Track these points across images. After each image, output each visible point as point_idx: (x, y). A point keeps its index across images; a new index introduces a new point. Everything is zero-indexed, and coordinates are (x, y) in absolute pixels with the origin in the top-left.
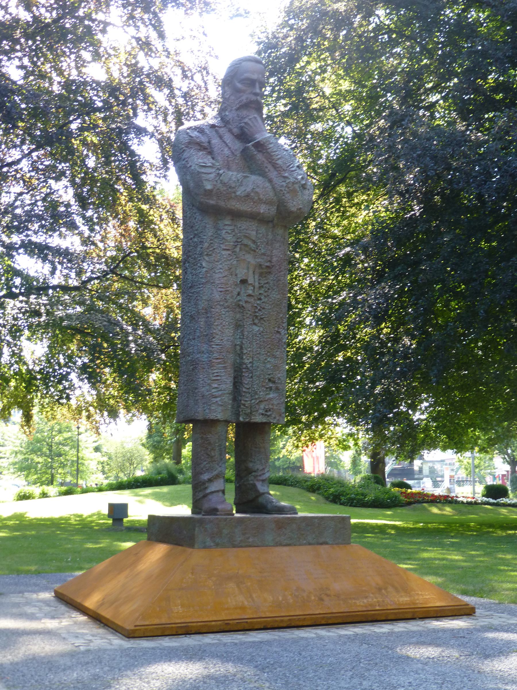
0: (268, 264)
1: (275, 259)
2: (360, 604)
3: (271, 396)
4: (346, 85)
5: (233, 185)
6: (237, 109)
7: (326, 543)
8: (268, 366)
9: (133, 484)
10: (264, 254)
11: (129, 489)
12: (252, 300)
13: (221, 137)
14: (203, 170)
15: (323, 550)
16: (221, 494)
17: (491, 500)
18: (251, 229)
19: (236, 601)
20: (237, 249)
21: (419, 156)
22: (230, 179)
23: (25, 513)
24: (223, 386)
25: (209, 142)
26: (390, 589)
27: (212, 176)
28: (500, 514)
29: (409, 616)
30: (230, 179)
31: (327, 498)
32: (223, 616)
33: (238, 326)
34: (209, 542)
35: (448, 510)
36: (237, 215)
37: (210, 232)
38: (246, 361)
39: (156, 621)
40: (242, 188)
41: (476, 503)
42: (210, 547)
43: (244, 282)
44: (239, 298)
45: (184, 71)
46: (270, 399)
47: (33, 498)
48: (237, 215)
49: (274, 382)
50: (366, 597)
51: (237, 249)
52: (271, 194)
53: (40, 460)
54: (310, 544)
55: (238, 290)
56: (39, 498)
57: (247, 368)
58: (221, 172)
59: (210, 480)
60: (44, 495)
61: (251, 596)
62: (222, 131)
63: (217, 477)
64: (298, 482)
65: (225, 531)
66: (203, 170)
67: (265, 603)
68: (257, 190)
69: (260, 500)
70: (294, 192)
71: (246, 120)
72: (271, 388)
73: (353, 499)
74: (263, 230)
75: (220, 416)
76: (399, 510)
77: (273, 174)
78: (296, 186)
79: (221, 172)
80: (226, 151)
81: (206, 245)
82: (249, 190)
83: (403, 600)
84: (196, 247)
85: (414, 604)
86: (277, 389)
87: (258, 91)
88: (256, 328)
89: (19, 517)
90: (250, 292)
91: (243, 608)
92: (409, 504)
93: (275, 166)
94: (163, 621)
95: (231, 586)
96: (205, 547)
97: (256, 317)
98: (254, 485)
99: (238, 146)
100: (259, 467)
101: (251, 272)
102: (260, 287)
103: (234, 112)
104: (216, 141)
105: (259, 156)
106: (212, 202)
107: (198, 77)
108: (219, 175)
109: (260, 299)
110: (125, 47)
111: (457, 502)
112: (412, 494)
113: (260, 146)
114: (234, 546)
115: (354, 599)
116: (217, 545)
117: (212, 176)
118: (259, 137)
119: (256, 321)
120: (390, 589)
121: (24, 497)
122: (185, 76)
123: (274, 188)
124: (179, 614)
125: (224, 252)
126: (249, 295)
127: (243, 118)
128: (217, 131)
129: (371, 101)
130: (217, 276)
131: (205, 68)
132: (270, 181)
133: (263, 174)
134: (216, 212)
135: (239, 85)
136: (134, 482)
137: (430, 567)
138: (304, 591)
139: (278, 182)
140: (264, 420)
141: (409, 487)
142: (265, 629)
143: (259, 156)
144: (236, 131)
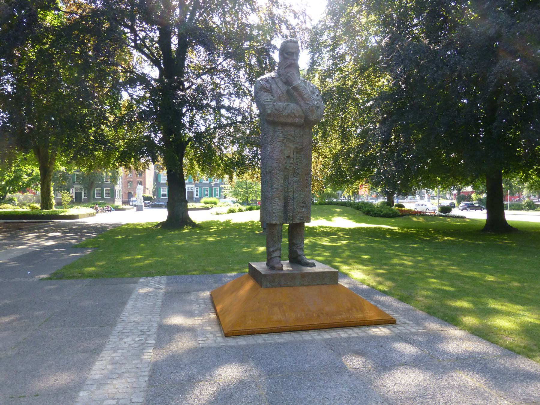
0: (301, 147)
1: (304, 144)
2: (338, 319)
4: (372, 17)
5: (281, 110)
6: (285, 68)
7: (326, 284)
8: (302, 196)
10: (299, 142)
12: (292, 165)
13: (276, 84)
14: (266, 103)
15: (324, 288)
16: (278, 258)
17: (443, 214)
18: (292, 131)
19: (278, 317)
20: (285, 141)
21: (402, 60)
22: (280, 107)
25: (271, 87)
26: (354, 310)
27: (271, 106)
28: (446, 221)
29: (362, 324)
30: (280, 107)
31: (364, 213)
32: (270, 326)
33: (286, 178)
34: (269, 285)
35: (421, 219)
36: (284, 124)
37: (271, 133)
38: (290, 195)
39: (238, 328)
40: (286, 111)
41: (435, 216)
42: (269, 287)
43: (288, 157)
44: (286, 165)
45: (295, 15)
46: (303, 212)
48: (284, 124)
49: (305, 204)
50: (341, 315)
51: (285, 141)
52: (301, 113)
53: (242, 190)
54: (318, 285)
55: (286, 161)
57: (291, 198)
58: (275, 104)
59: (273, 251)
60: (240, 210)
61: (285, 315)
62: (278, 80)
63: (276, 250)
64: (351, 205)
65: (277, 280)
66: (266, 103)
67: (291, 318)
68: (294, 111)
69: (299, 258)
70: (313, 111)
71: (289, 74)
72: (303, 207)
73: (376, 213)
74: (298, 130)
75: (277, 222)
76: (397, 219)
77: (302, 103)
78: (314, 108)
79: (275, 104)
80: (279, 91)
81: (269, 140)
82: (289, 112)
83: (360, 316)
84: (265, 140)
85: (365, 318)
86: (306, 207)
88: (295, 179)
89: (227, 223)
91: (280, 321)
92: (403, 216)
93: (303, 98)
94: (242, 328)
95: (276, 309)
96: (267, 287)
98: (296, 251)
99: (284, 88)
100: (298, 242)
101: (292, 152)
102: (297, 159)
103: (283, 69)
104: (274, 86)
106: (271, 119)
107: (301, 17)
110: (266, 4)
111: (426, 215)
112: (405, 210)
113: (295, 89)
114: (281, 287)
115: (335, 316)
116: (273, 286)
117: (271, 106)
119: (295, 175)
120: (354, 310)
121: (231, 211)
122: (295, 17)
123: (302, 109)
124: (250, 324)
125: (278, 143)
126: (291, 163)
127: (288, 73)
128: (275, 81)
129: (386, 23)
130: (275, 155)
131: (305, 13)
132: (301, 106)
133: (297, 103)
134: (274, 124)
137: (392, 273)
138: (311, 311)
139: (305, 107)
141: (403, 206)
143: (295, 94)
144: (284, 80)
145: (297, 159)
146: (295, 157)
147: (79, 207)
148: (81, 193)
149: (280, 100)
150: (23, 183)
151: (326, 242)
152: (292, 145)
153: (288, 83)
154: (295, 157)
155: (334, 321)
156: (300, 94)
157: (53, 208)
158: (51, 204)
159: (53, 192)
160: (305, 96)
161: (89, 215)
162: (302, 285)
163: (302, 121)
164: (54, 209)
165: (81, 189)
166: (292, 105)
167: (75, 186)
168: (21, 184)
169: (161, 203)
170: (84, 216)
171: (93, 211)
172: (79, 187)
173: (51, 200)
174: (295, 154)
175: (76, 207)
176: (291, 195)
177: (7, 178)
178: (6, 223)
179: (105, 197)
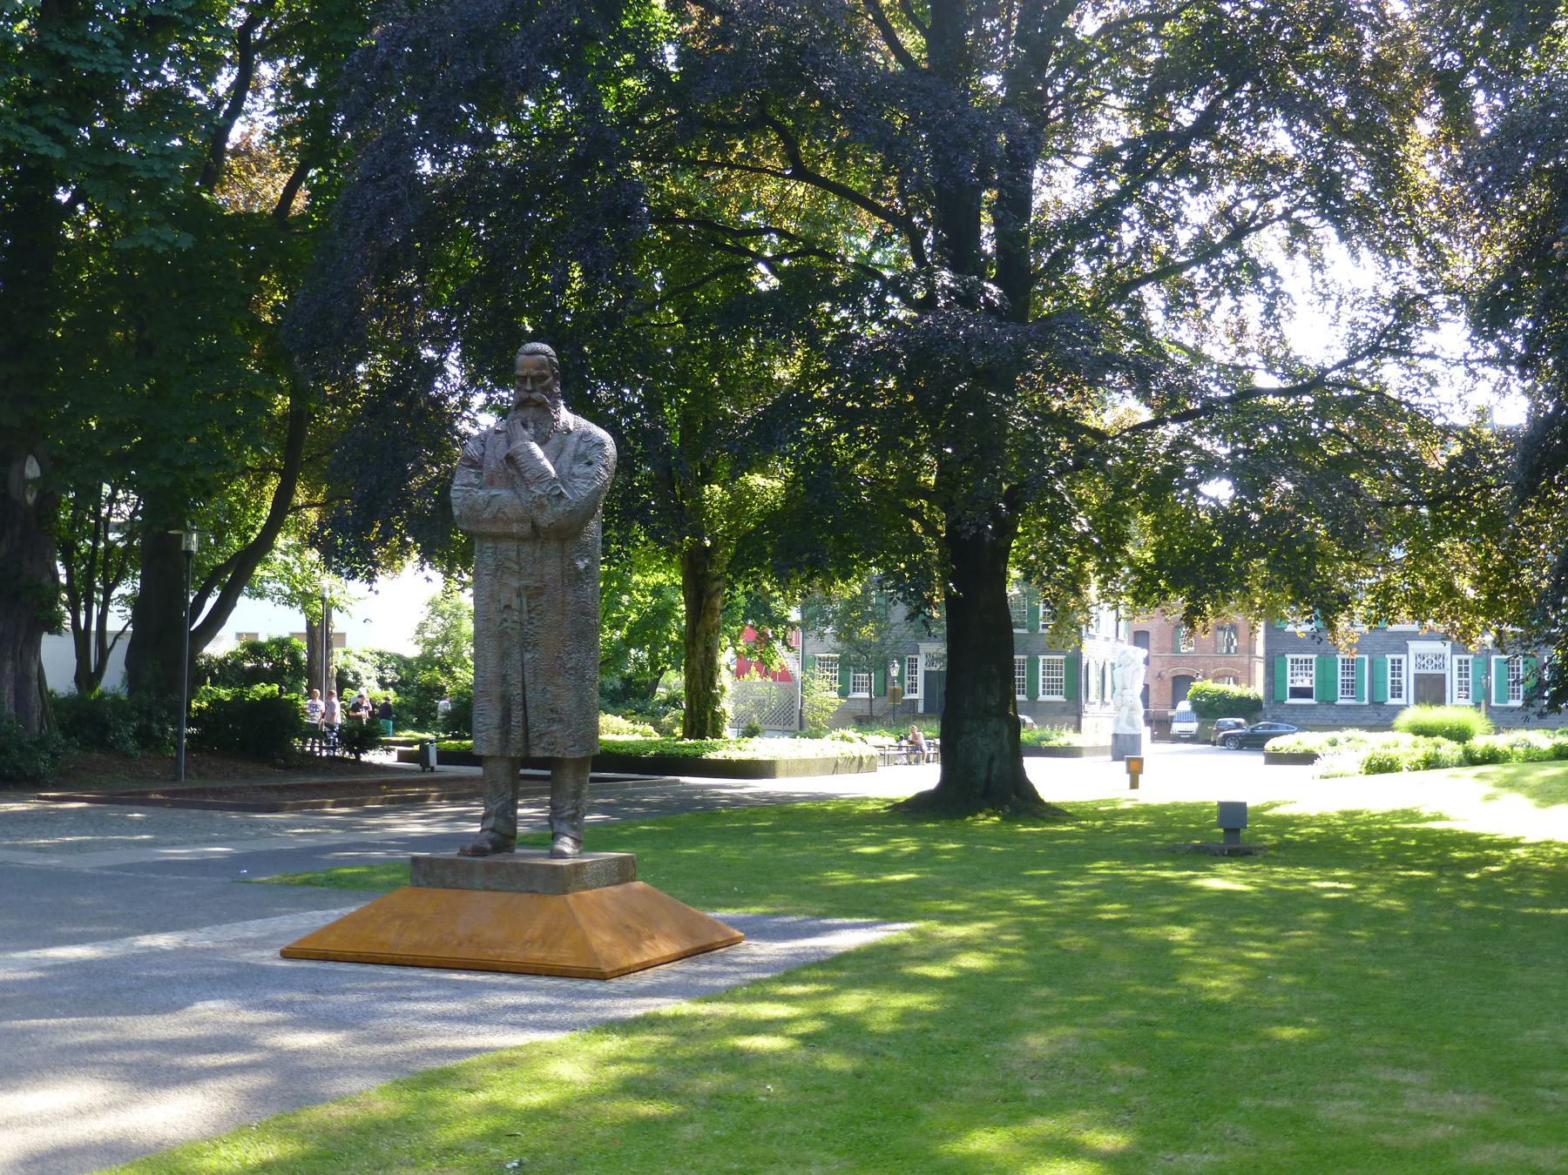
2: (489, 954)
18: (509, 548)
24: (488, 721)
36: (496, 538)
43: (508, 607)
60: (1431, 763)
72: (554, 720)
74: (527, 548)
88: (528, 656)
113: (510, 459)
116: (429, 884)
140: (547, 754)
151: (1330, 884)
156: (518, 470)
157: (729, 732)
158: (718, 718)
160: (527, 475)
162: (487, 889)
163: (527, 528)
166: (505, 493)
170: (804, 767)
173: (716, 702)
176: (516, 691)
177: (633, 616)
179: (1042, 698)
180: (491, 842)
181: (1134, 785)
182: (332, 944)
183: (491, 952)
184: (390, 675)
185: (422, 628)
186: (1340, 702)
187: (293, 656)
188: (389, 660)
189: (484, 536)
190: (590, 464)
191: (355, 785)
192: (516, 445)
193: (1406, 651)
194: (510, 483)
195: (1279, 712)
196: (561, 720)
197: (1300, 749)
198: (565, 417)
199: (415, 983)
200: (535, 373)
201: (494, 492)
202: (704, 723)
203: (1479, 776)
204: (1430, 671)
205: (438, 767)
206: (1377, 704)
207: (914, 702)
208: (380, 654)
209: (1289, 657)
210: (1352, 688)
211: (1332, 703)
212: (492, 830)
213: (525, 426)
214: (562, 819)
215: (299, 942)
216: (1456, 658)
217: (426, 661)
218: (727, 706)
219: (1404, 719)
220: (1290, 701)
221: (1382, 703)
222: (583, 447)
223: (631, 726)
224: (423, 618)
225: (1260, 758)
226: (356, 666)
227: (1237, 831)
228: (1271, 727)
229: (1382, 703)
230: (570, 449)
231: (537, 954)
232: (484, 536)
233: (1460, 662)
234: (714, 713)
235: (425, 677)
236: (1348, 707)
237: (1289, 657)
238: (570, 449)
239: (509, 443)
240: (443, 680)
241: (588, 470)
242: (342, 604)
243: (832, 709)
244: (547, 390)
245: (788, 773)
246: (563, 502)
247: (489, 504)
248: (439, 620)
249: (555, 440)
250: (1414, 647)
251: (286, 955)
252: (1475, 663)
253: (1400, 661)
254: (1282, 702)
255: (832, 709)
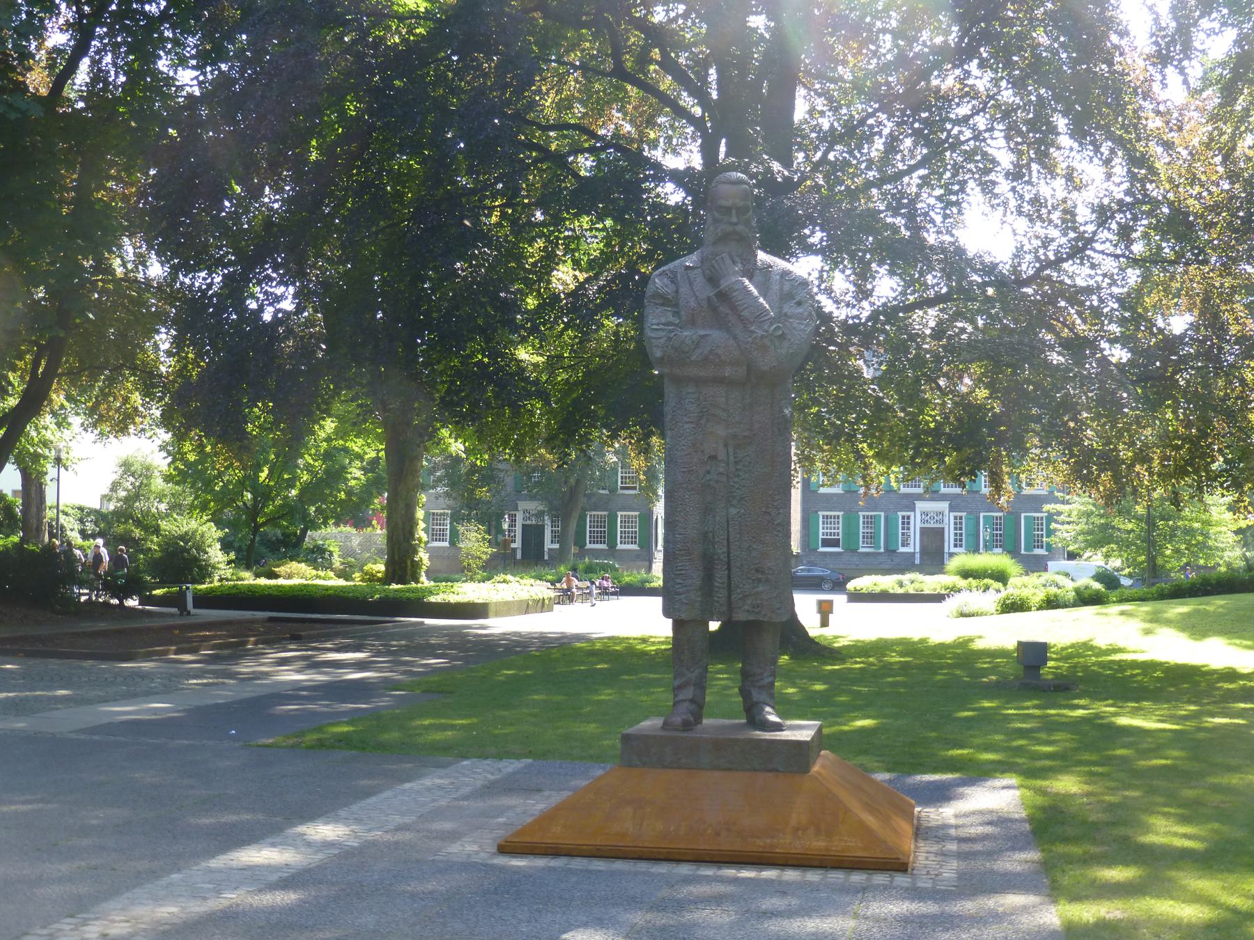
2: (759, 844)
3: (760, 589)
6: (714, 243)
7: (777, 771)
8: (754, 554)
9: (1199, 589)
11: (1191, 596)
13: (691, 284)
23: (971, 640)
24: (689, 582)
25: (677, 292)
27: (662, 341)
29: (816, 863)
33: (707, 510)
36: (699, 382)
39: (528, 839)
40: (699, 351)
43: (713, 458)
44: (708, 477)
47: (1029, 609)
49: (763, 573)
51: (703, 421)
56: (1040, 608)
57: (719, 559)
68: (719, 351)
72: (759, 581)
80: (692, 304)
86: (767, 581)
87: (734, 220)
88: (733, 511)
90: (721, 470)
93: (742, 319)
94: (535, 840)
96: (630, 766)
97: (734, 497)
104: (684, 290)
105: (724, 309)
108: (670, 339)
109: (738, 476)
113: (723, 296)
114: (664, 767)
117: (662, 341)
118: (724, 284)
119: (735, 502)
132: (735, 337)
133: (728, 330)
135: (716, 214)
136: (1202, 584)
140: (751, 618)
142: (640, 858)
143: (724, 309)
145: (736, 463)
146: (732, 458)
147: (509, 577)
148: (541, 529)
149: (692, 322)
150: (349, 493)
152: (721, 431)
153: (713, 280)
154: (732, 458)
155: (749, 849)
156: (734, 308)
157: (423, 578)
158: (417, 566)
159: (422, 525)
160: (745, 313)
161: (528, 607)
162: (716, 768)
164: (425, 582)
165: (540, 514)
166: (716, 335)
167: (522, 505)
168: (343, 495)
169: (818, 572)
171: (542, 590)
172: (533, 506)
173: (416, 552)
174: (731, 450)
175: (502, 577)
176: (721, 550)
177: (305, 477)
178: (271, 619)
179: (620, 547)
180: (692, 713)
181: (825, 623)
182: (557, 834)
183: (759, 842)
184: (90, 527)
185: (115, 487)
186: (861, 550)
187: (8, 509)
188: (89, 514)
189: (679, 381)
190: (799, 304)
191: (149, 629)
192: (724, 284)
193: (914, 510)
194: (720, 323)
195: (813, 558)
196: (767, 581)
197: (878, 590)
198: (762, 256)
199: (729, 889)
200: (742, 204)
201: (702, 332)
202: (404, 569)
203: (1122, 613)
204: (932, 525)
205: (193, 611)
206: (891, 552)
207: (514, 550)
208: (81, 509)
209: (821, 514)
210: (872, 538)
211: (855, 551)
212: (692, 701)
213: (734, 262)
214: (761, 687)
215: (518, 833)
216: (952, 514)
217: (122, 515)
218: (423, 556)
219: (953, 564)
220: (822, 549)
221: (894, 551)
222: (787, 287)
223: (314, 572)
224: (115, 477)
225: (845, 597)
226: (63, 519)
227: (1038, 668)
228: (809, 571)
229: (894, 551)
230: (776, 287)
231: (817, 844)
232: (679, 381)
233: (955, 518)
234: (413, 561)
235: (120, 529)
236: (867, 554)
237: (821, 514)
238: (776, 287)
239: (713, 280)
240: (137, 533)
241: (801, 310)
242: (69, 463)
243: (484, 557)
244: (747, 223)
245: (497, 614)
246: (786, 344)
247: (697, 345)
248: (131, 479)
249: (758, 277)
250: (920, 506)
251: (504, 849)
252: (967, 519)
253: (909, 517)
254: (815, 550)
255: (484, 557)
